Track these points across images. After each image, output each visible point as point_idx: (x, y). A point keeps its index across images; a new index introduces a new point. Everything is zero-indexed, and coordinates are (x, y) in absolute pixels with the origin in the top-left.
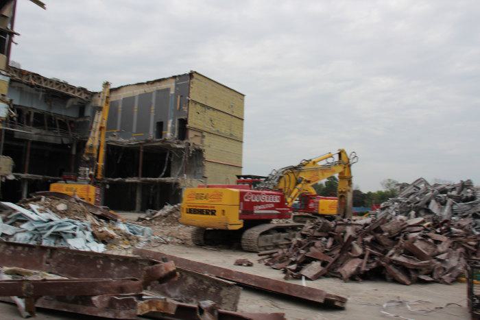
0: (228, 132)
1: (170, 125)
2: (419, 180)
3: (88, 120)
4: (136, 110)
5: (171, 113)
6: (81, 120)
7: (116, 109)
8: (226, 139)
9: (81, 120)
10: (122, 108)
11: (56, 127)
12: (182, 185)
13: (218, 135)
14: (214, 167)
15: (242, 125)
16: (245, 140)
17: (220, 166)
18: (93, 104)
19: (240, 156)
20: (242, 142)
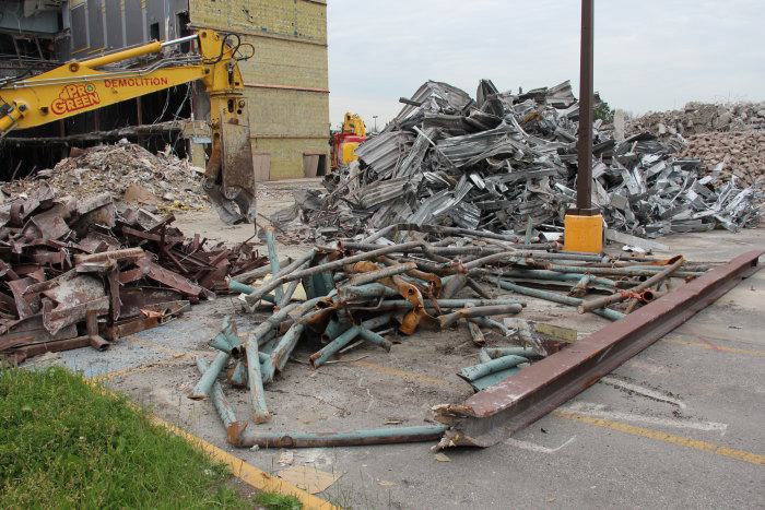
0: (290, 30)
1: (167, 29)
2: (425, 85)
3: (68, 34)
4: (123, 8)
5: (167, 7)
6: (60, 37)
7: (99, 12)
8: (286, 44)
9: (60, 37)
10: (106, 6)
11: (15, 53)
12: (186, 134)
13: (266, 36)
14: (260, 95)
15: (323, 15)
16: (331, 38)
17: (273, 94)
18: (69, 6)
19: (322, 72)
20: (326, 46)
